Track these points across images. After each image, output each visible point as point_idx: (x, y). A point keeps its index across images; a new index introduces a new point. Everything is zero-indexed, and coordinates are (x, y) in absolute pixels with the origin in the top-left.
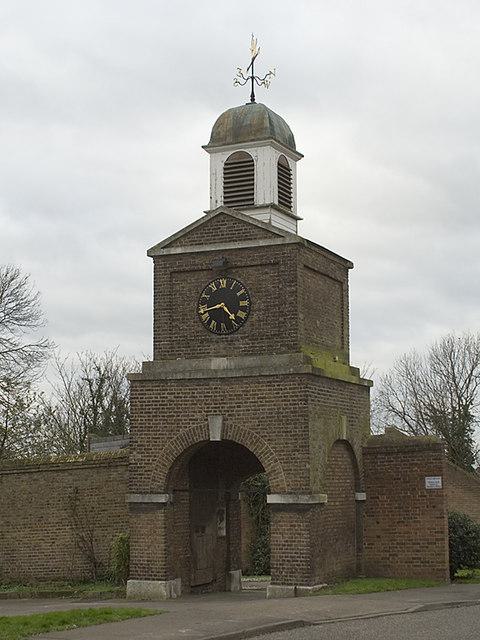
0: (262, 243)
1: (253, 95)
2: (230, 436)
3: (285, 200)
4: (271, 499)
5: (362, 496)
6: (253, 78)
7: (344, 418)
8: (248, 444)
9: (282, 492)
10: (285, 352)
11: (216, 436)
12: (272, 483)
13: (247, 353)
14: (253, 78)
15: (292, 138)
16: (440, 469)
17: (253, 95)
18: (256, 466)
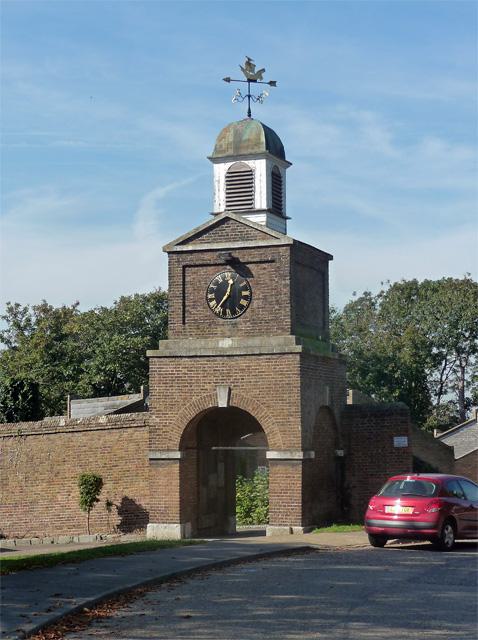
0: (261, 244)
1: (249, 112)
2: (235, 403)
3: (276, 208)
4: (270, 455)
5: (341, 453)
6: (249, 96)
7: (328, 388)
8: (249, 409)
9: (279, 450)
10: (280, 334)
11: (223, 403)
12: (271, 441)
13: (249, 334)
14: (249, 96)
15: (396, 287)
16: (407, 431)
17: (249, 112)
18: (254, 426)
